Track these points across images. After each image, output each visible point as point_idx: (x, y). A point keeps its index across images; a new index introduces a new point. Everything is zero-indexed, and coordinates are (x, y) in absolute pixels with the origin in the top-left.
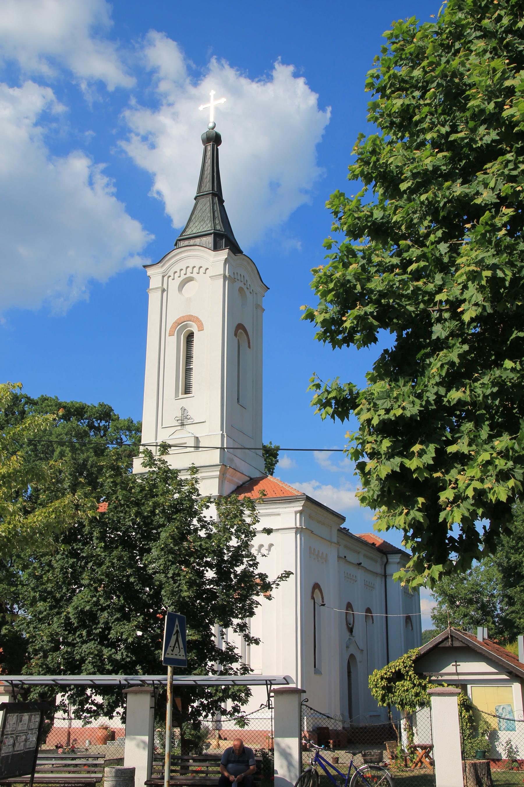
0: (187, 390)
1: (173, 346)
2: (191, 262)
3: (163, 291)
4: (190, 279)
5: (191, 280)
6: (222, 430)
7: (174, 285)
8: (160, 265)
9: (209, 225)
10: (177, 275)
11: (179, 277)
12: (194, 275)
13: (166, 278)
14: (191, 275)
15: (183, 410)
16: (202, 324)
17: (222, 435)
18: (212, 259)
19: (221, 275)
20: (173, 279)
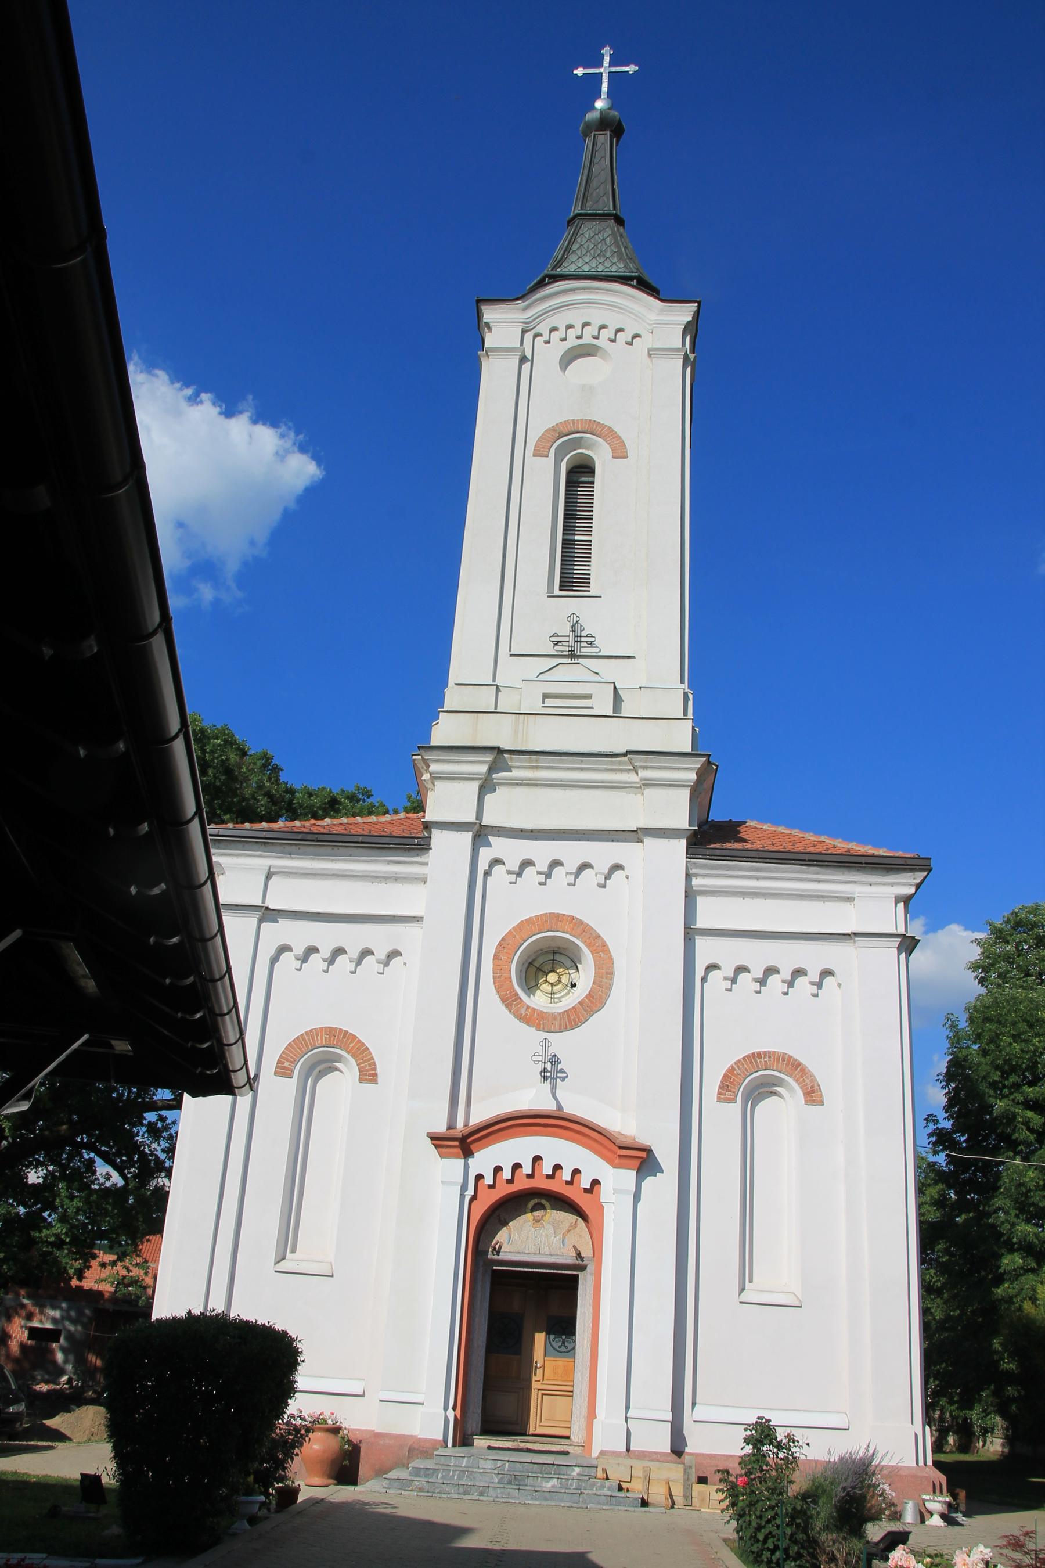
1: (543, 483)
2: (597, 317)
3: (523, 360)
4: (587, 351)
5: (589, 355)
6: (682, 681)
7: (547, 355)
8: (522, 304)
9: (622, 265)
10: (560, 333)
11: (564, 340)
12: (603, 342)
13: (529, 336)
14: (595, 342)
17: (685, 694)
18: (653, 317)
19: (677, 350)
20: (547, 342)
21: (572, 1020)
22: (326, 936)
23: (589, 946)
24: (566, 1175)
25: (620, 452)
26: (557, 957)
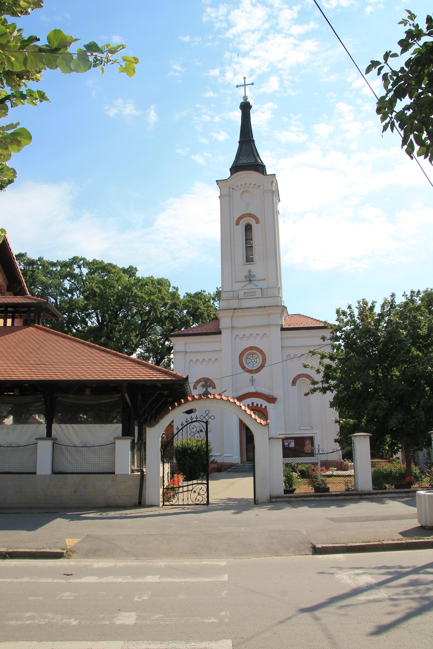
0: (249, 260)
13: (231, 189)
15: (250, 271)
16: (258, 220)
21: (258, 370)
22: (200, 357)
23: (260, 353)
24: (259, 406)
25: (257, 222)
26: (254, 355)
